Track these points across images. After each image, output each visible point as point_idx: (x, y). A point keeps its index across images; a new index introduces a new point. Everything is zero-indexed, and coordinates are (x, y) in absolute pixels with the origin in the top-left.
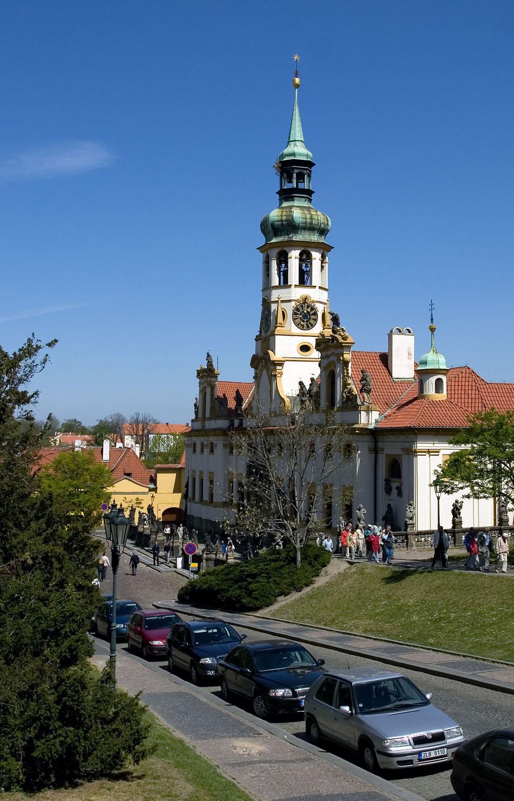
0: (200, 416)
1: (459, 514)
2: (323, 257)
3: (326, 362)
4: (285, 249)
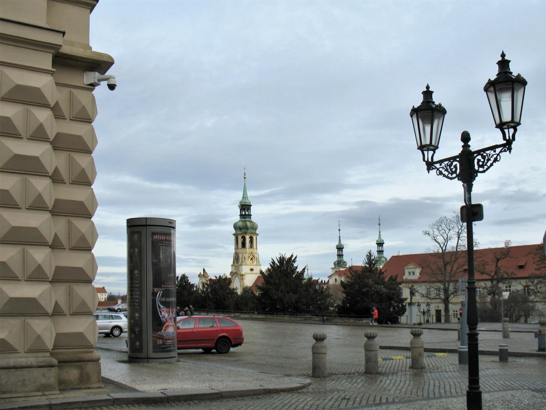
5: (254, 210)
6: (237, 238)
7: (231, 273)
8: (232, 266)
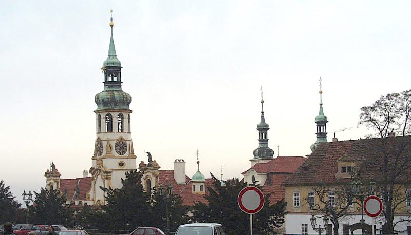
4: (111, 113)
7: (92, 169)
8: (93, 158)
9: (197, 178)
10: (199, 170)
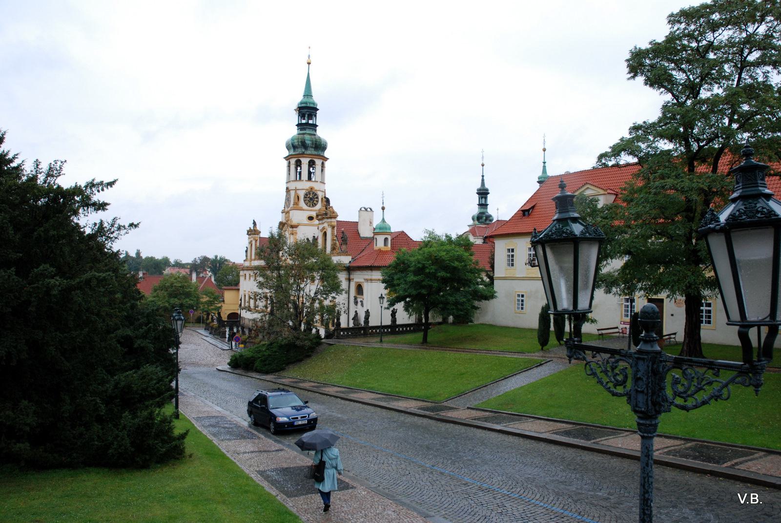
0: (249, 257)
1: (395, 316)
2: (323, 164)
3: (321, 227)
5: (320, 119)
6: (289, 163)
9: (380, 229)
10: (383, 219)
